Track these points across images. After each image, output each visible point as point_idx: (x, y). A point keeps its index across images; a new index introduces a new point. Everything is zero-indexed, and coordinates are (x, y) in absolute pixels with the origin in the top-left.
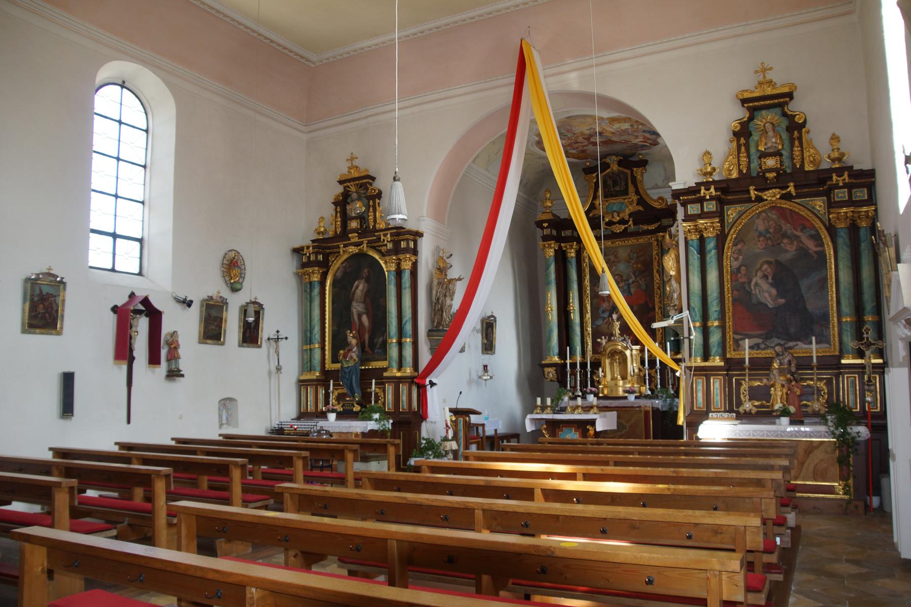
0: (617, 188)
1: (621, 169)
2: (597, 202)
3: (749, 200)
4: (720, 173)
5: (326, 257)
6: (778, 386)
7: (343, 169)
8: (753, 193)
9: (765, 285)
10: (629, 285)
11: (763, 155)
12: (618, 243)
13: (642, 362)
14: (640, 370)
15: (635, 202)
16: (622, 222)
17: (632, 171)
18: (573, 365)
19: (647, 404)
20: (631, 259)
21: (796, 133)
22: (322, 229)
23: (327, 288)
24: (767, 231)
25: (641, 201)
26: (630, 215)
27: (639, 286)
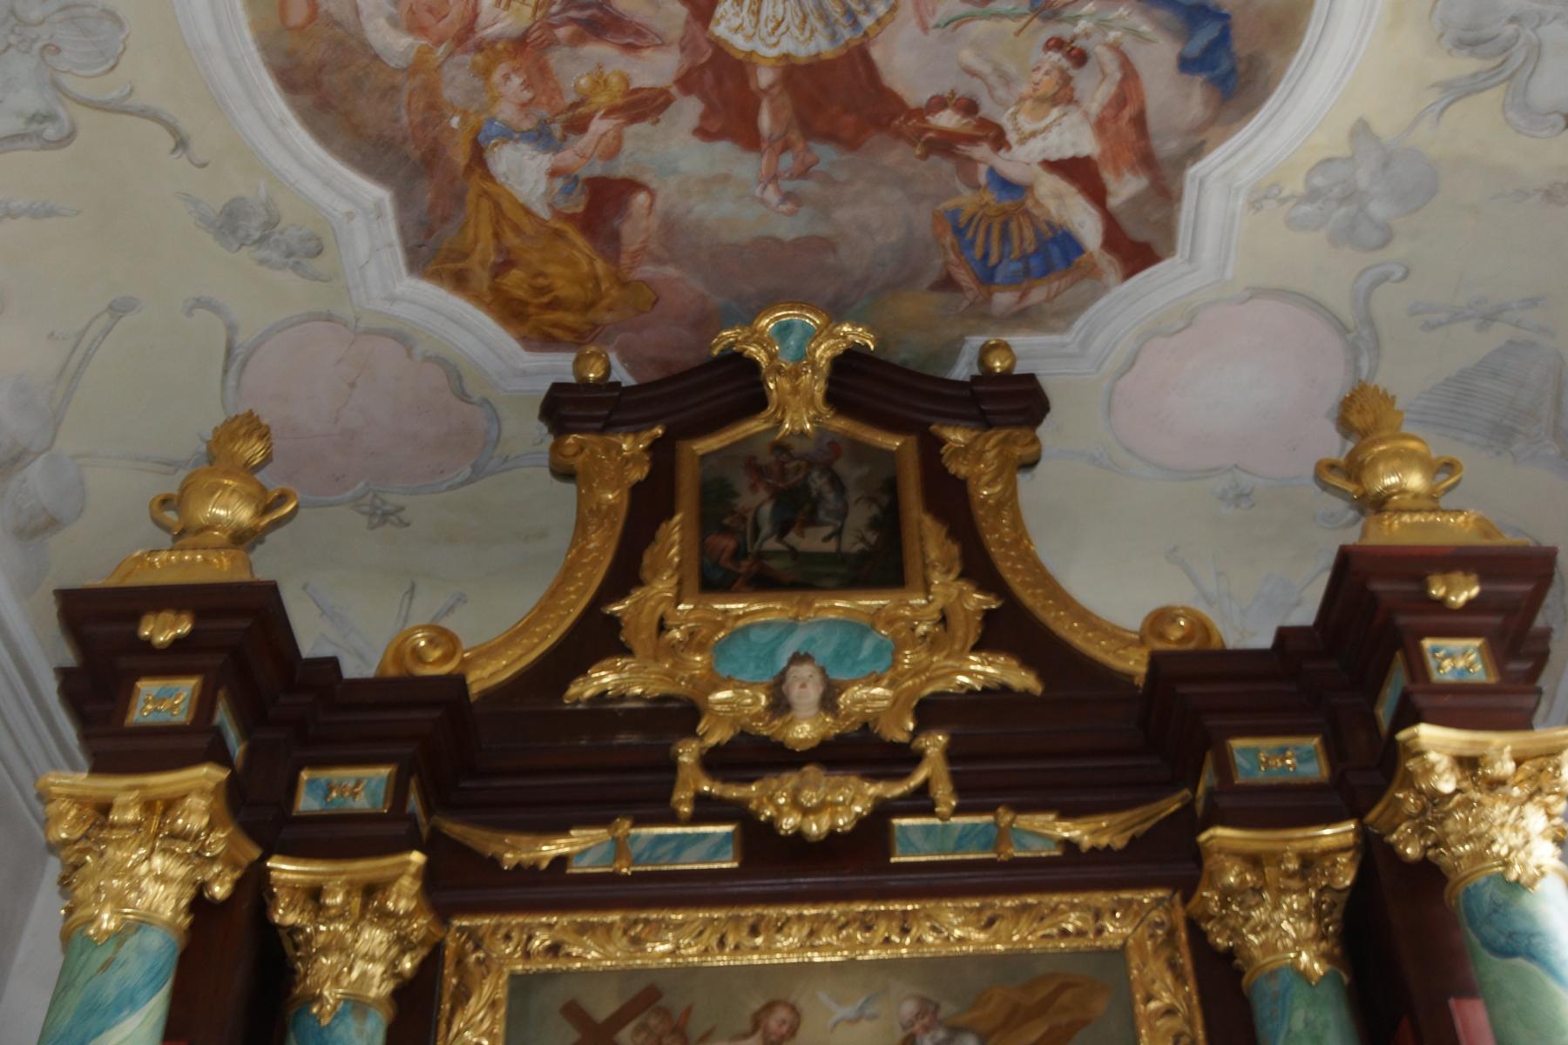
0: (813, 541)
1: (841, 424)
17: (931, 447)
25: (1009, 628)
26: (931, 711)
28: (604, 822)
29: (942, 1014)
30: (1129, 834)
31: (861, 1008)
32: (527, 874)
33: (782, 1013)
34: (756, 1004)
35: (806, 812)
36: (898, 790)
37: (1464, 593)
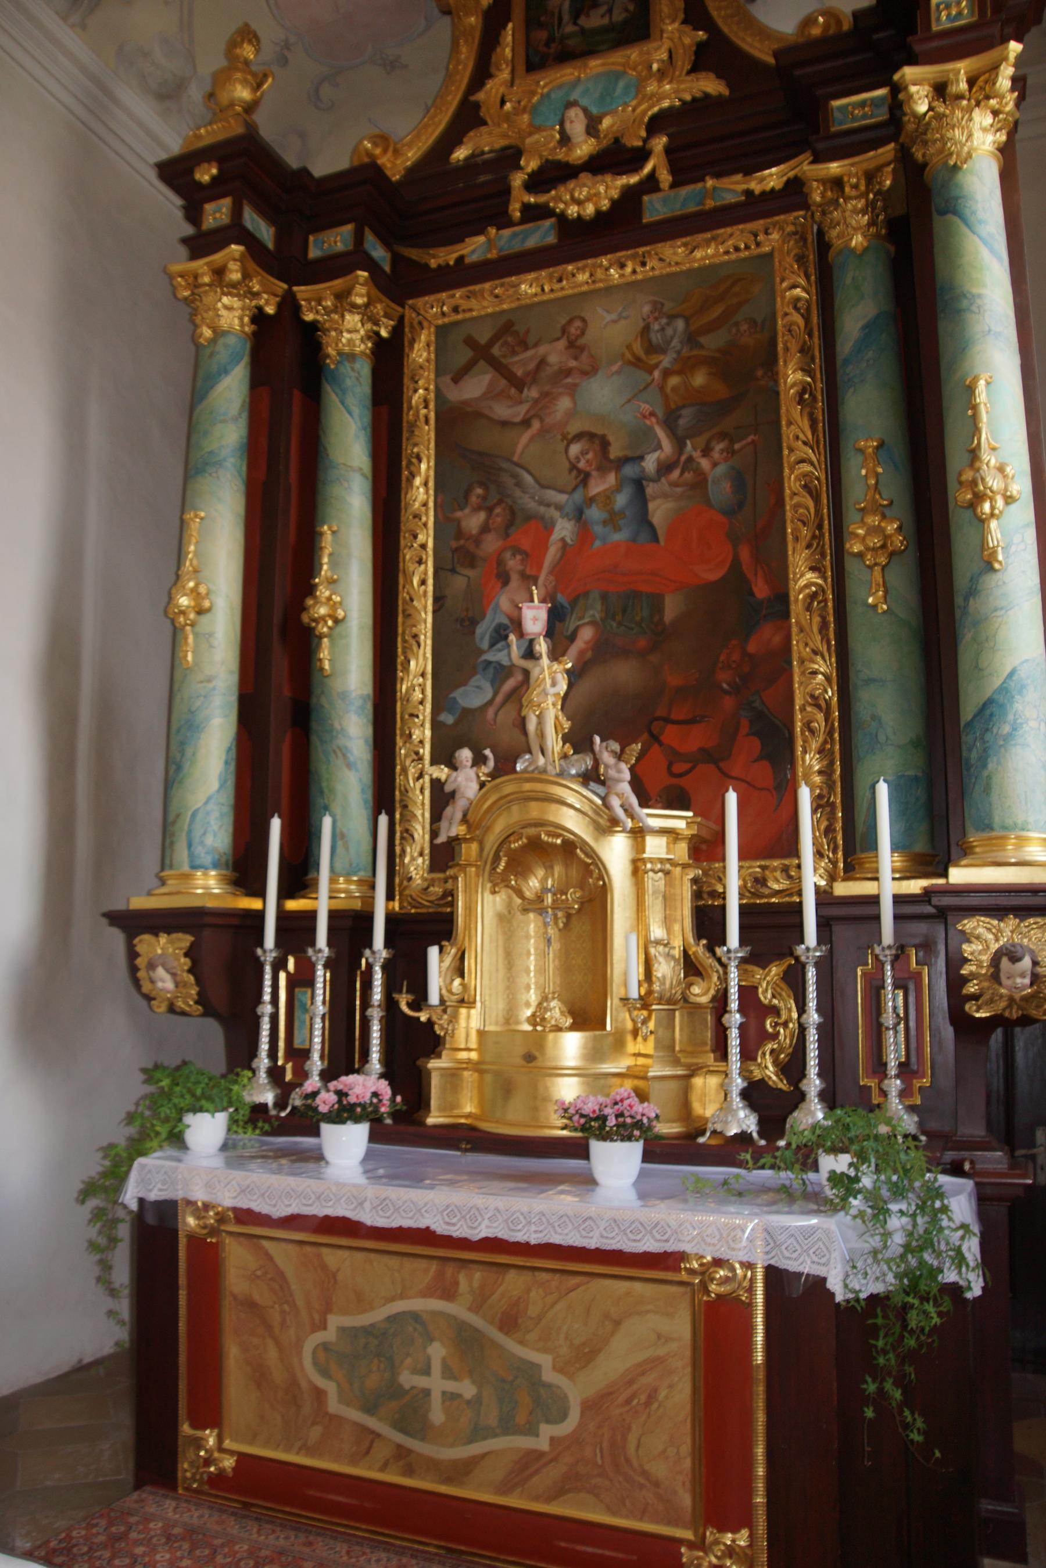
0: (595, 20)
10: (639, 485)
13: (708, 922)
14: (691, 968)
15: (684, 63)
16: (614, 158)
18: (296, 931)
19: (741, 1234)
20: (652, 349)
27: (700, 483)
28: (481, 232)
29: (666, 309)
30: (785, 178)
31: (620, 315)
32: (443, 269)
33: (578, 324)
34: (564, 322)
35: (579, 203)
36: (634, 179)
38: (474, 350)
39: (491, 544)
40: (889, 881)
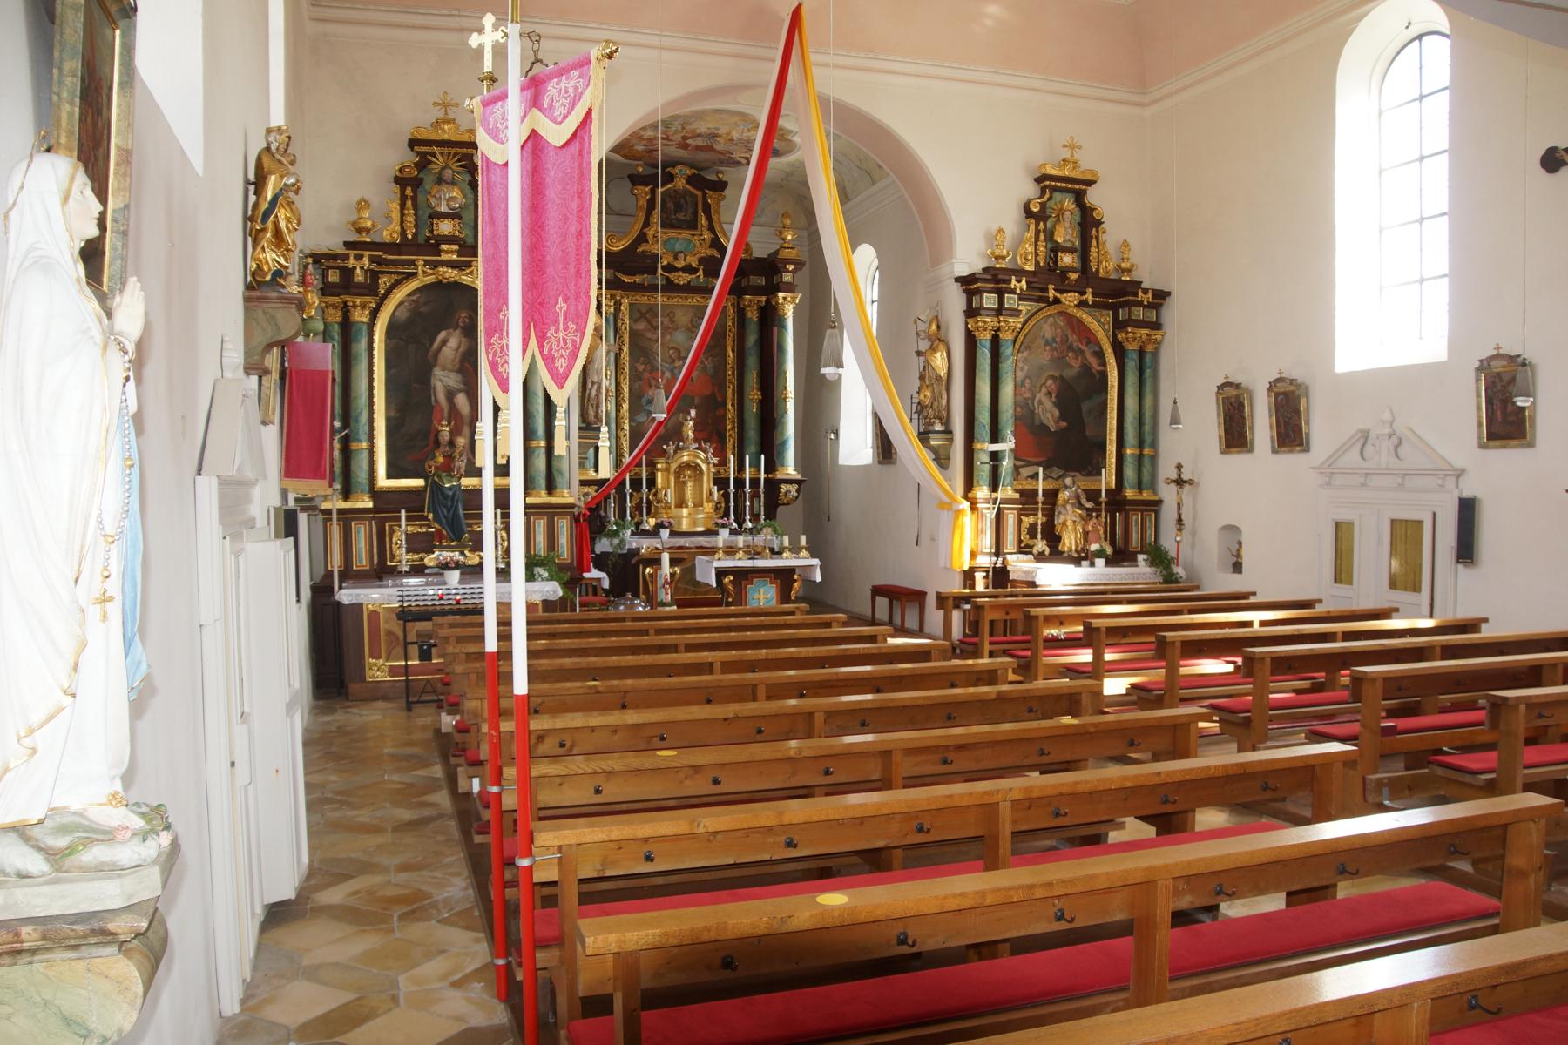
0: (681, 216)
2: (650, 233)
3: (1044, 300)
4: (1015, 258)
5: (375, 275)
6: (1069, 523)
7: (417, 117)
8: (1052, 293)
9: (1048, 404)
11: (1055, 250)
12: (677, 300)
15: (708, 243)
16: (689, 269)
21: (1094, 232)
22: (369, 224)
23: (376, 338)
24: (1054, 339)
26: (701, 261)
37: (791, 267)
38: (639, 314)
39: (646, 375)
40: (763, 476)
